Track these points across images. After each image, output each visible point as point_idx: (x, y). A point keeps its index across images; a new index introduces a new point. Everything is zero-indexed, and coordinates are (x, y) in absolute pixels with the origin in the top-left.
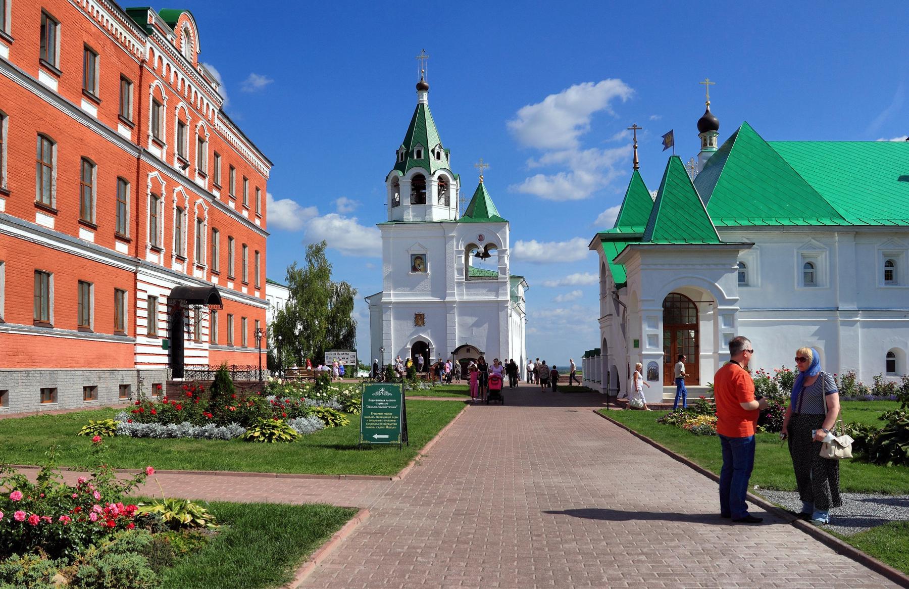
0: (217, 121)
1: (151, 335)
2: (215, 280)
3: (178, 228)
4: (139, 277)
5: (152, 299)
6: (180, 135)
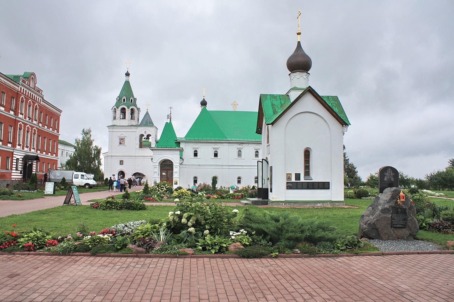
0: (41, 102)
1: (17, 170)
2: (39, 152)
3: (27, 137)
4: (14, 153)
5: (17, 159)
6: (29, 109)
